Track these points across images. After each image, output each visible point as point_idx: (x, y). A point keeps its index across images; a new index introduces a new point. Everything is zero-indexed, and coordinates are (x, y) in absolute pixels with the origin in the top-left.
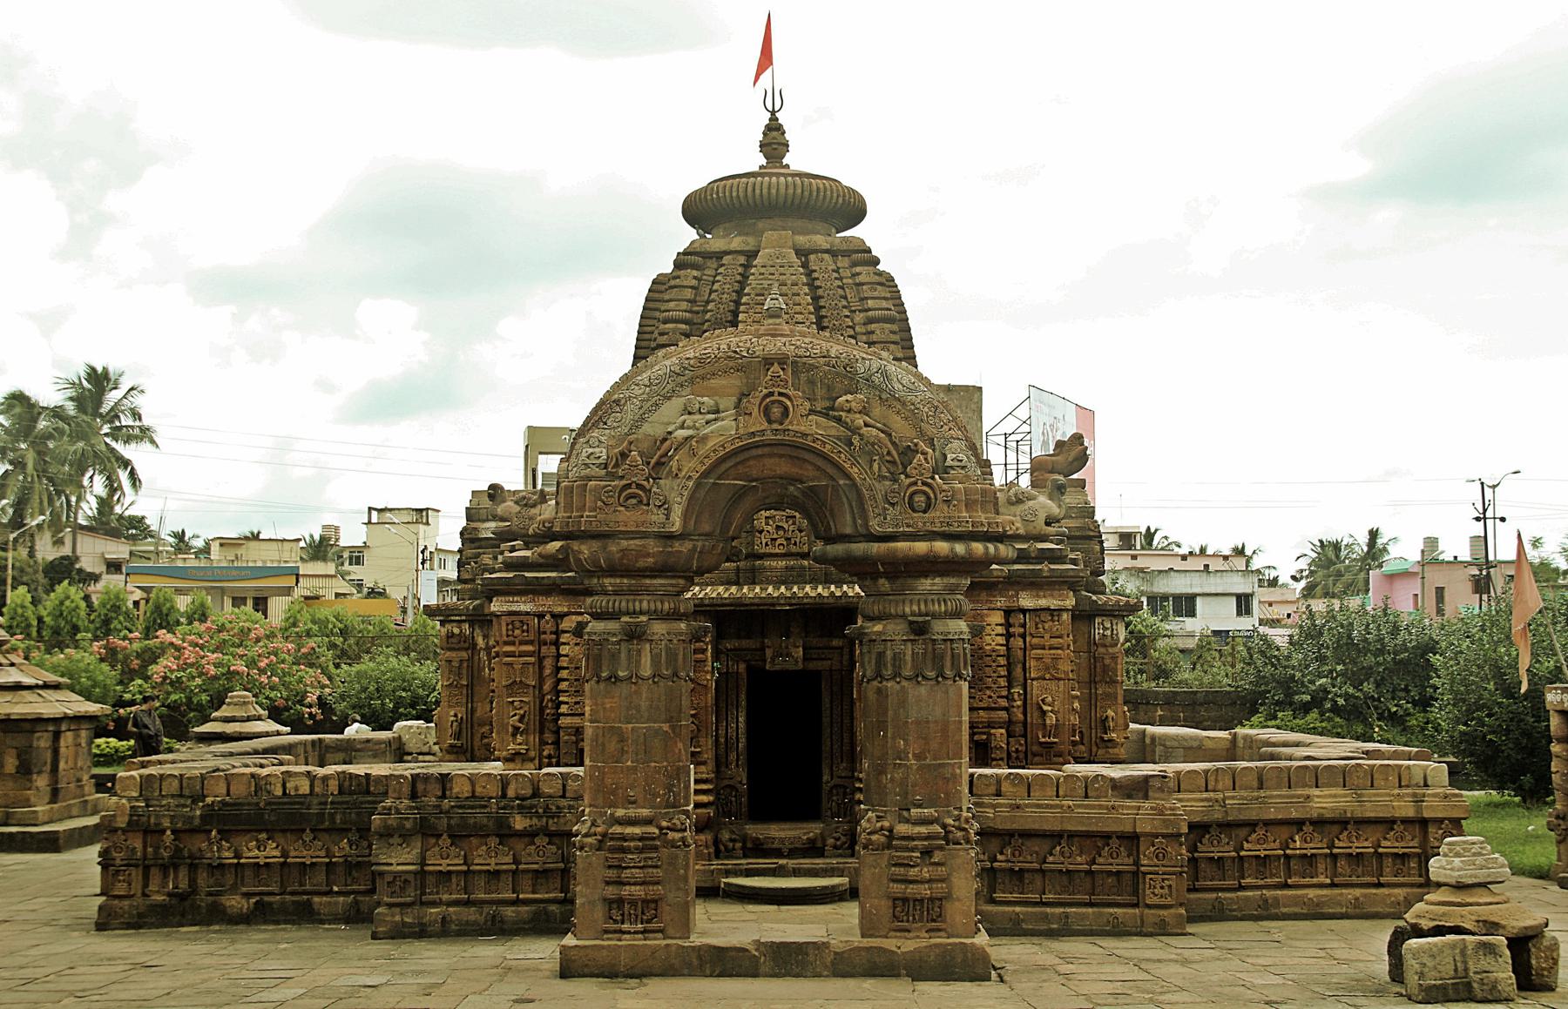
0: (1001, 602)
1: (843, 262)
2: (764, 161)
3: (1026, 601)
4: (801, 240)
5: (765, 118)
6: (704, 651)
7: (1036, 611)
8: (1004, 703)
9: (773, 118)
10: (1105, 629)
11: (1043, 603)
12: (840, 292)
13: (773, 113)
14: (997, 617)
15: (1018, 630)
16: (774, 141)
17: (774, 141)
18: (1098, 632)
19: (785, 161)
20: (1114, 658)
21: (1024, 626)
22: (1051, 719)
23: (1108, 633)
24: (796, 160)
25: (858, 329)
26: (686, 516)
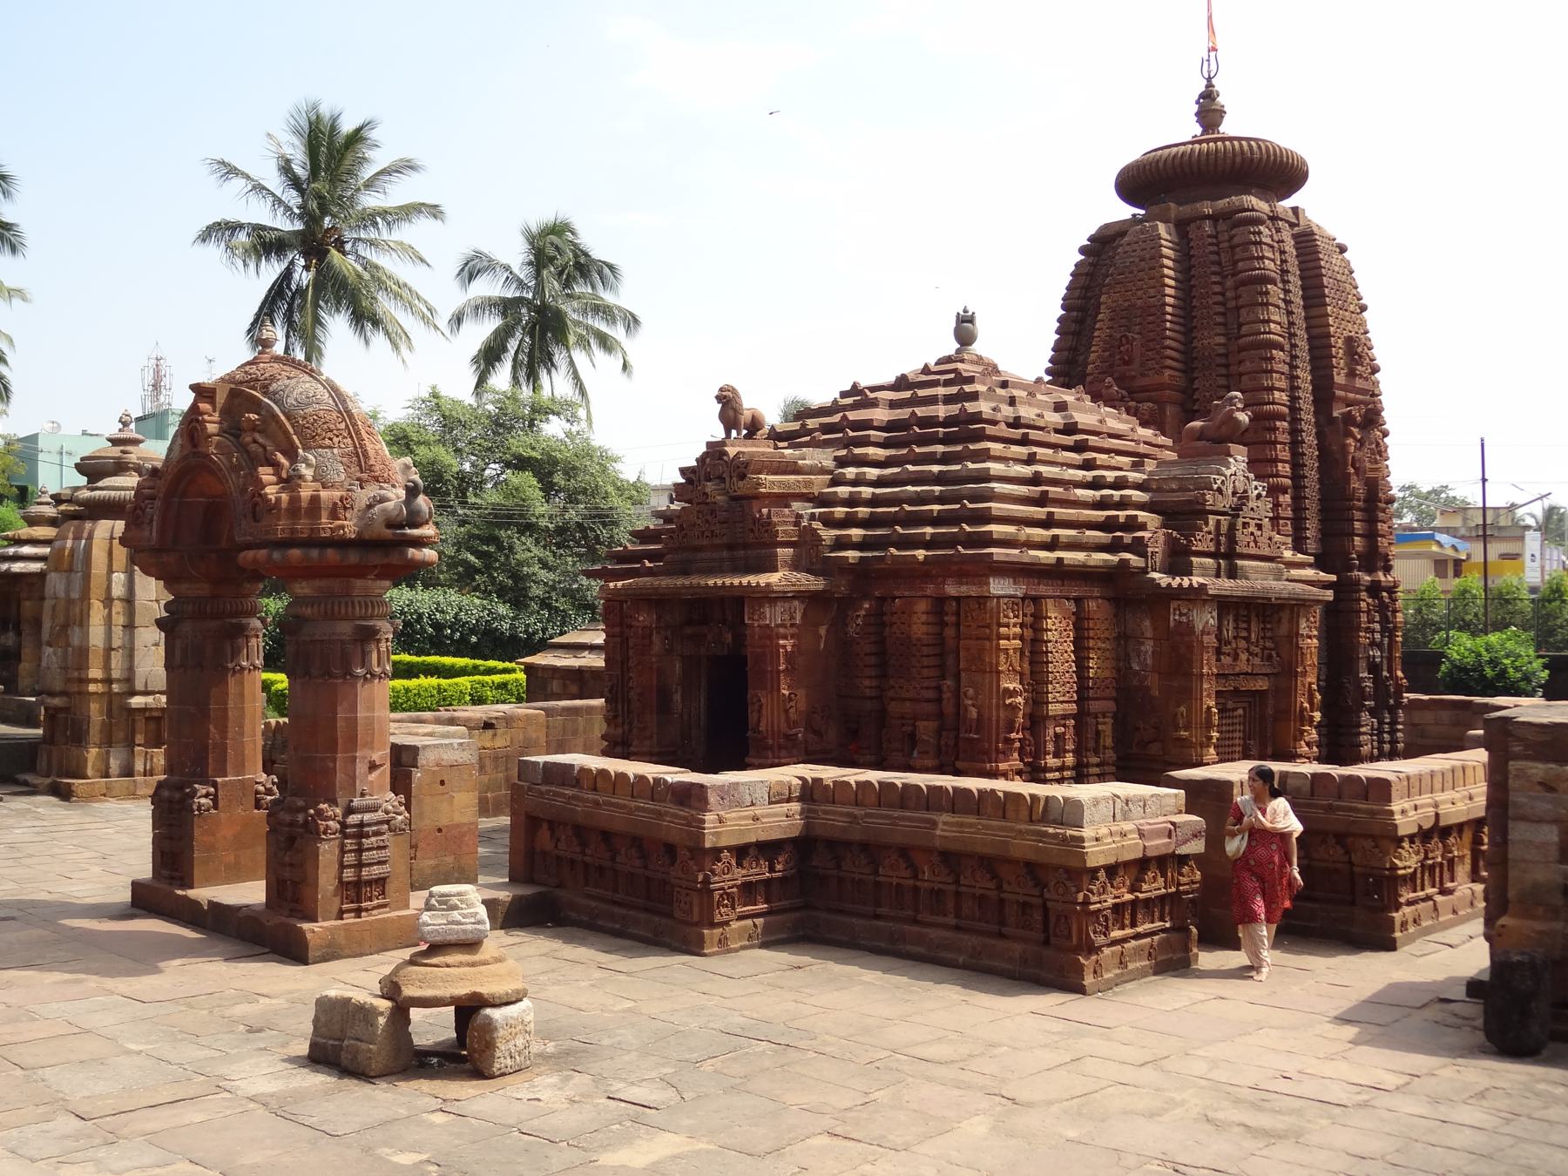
0: (930, 589)
1: (1222, 226)
2: (1198, 130)
3: (952, 589)
4: (1186, 210)
5: (1201, 87)
6: (651, 635)
7: (958, 599)
8: (930, 694)
9: (1210, 85)
10: (1181, 615)
11: (964, 590)
12: (1214, 258)
13: (1209, 79)
14: (922, 606)
15: (950, 619)
16: (1209, 110)
17: (1209, 110)
18: (1174, 617)
19: (1221, 129)
20: (1190, 647)
21: (958, 614)
22: (974, 713)
23: (1184, 619)
24: (1230, 127)
25: (1229, 294)
26: (162, 531)
